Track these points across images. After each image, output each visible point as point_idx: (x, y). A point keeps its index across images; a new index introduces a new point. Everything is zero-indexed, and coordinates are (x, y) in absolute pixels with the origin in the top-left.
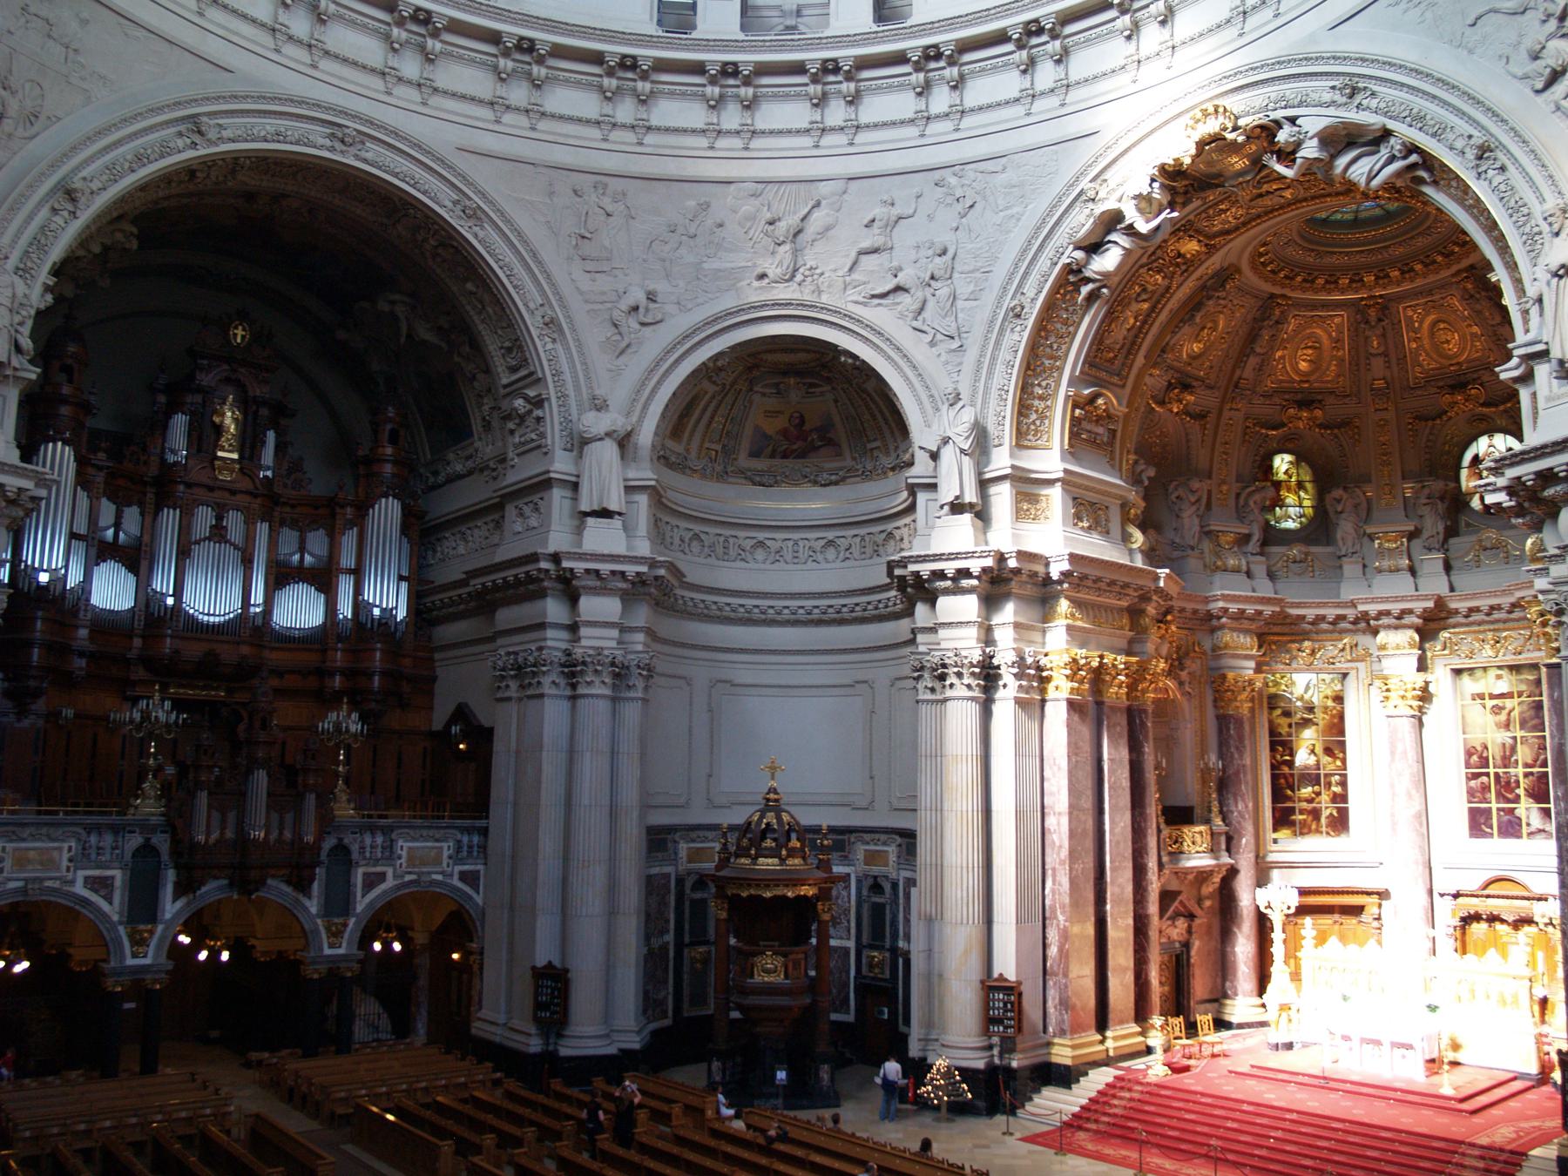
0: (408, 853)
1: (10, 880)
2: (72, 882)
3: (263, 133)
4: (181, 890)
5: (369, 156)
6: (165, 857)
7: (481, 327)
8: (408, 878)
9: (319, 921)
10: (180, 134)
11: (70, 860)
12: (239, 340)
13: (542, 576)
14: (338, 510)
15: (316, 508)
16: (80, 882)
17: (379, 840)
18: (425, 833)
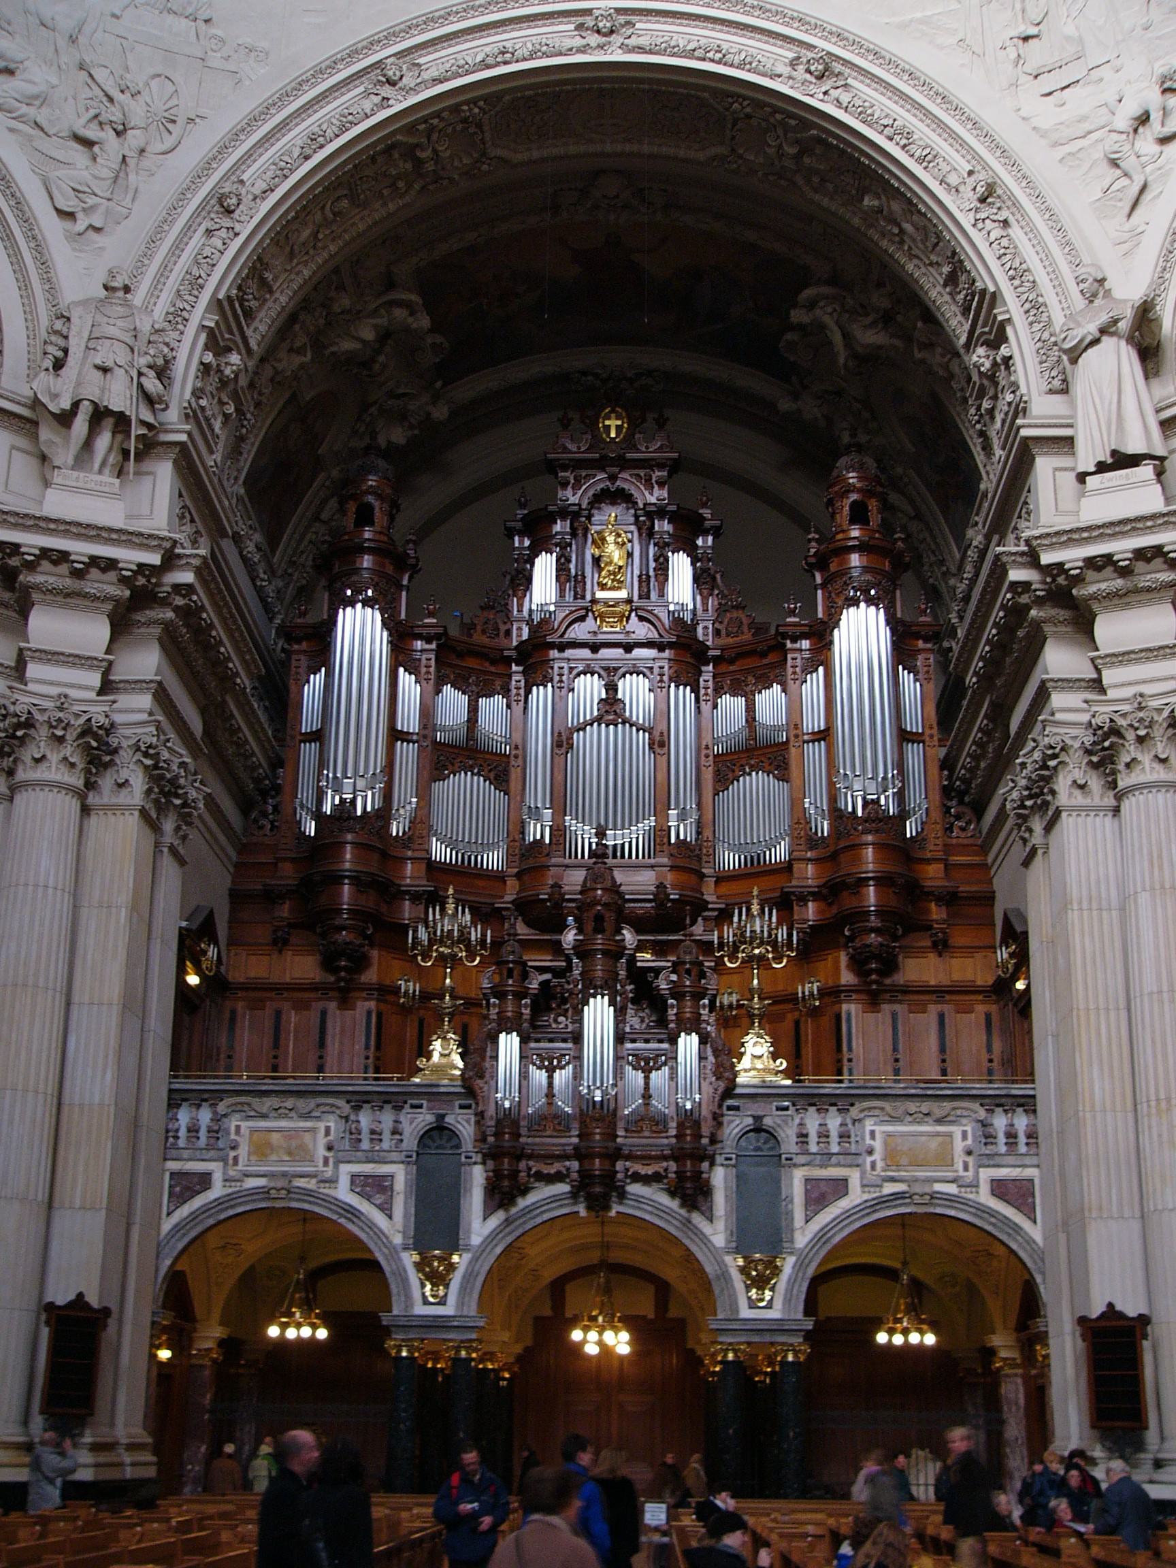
0: (886, 1143)
2: (333, 1181)
3: (479, 59)
5: (643, 41)
7: (910, 267)
8: (889, 1188)
9: (728, 1259)
10: (367, 94)
11: (330, 1148)
12: (613, 435)
13: (1024, 599)
14: (789, 645)
15: (763, 655)
16: (344, 1181)
17: (834, 1122)
18: (912, 1106)
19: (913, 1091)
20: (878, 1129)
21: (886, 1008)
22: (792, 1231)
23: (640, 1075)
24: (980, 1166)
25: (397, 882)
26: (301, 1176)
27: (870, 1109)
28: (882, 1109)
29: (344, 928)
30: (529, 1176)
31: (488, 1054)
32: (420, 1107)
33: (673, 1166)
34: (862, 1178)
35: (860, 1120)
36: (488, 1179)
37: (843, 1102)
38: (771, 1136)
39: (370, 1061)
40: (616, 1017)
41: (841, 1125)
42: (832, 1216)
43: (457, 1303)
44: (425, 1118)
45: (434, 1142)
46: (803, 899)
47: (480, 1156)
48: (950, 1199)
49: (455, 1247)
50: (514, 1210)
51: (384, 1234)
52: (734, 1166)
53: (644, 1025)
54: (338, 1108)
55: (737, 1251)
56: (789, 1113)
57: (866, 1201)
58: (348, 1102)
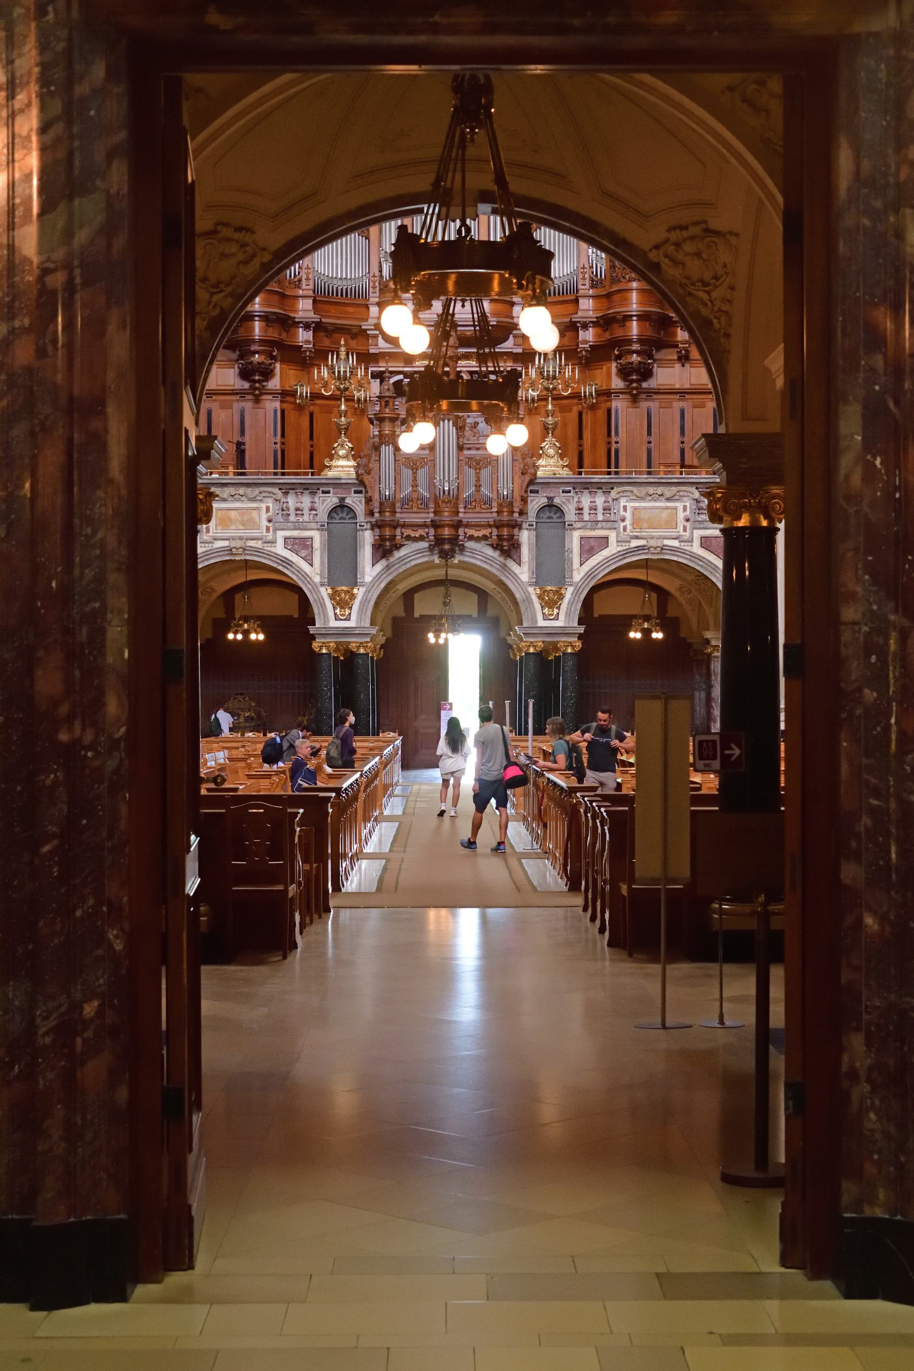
1: (216, 539)
2: (273, 542)
4: (383, 550)
6: (361, 518)
8: (635, 543)
9: (531, 589)
11: (270, 521)
16: (280, 542)
17: (600, 500)
18: (651, 490)
19: (652, 480)
20: (628, 505)
21: (644, 405)
22: (572, 571)
23: (473, 471)
24: (695, 528)
25: (292, 315)
26: (252, 539)
27: (623, 492)
28: (632, 492)
29: (257, 352)
30: (402, 537)
31: (374, 458)
32: (328, 492)
33: (495, 532)
34: (617, 537)
35: (616, 499)
36: (375, 540)
37: (605, 488)
38: (559, 510)
39: (278, 446)
40: (457, 434)
41: (604, 502)
42: (598, 561)
43: (357, 618)
44: (332, 500)
45: (338, 514)
46: (585, 326)
47: (369, 525)
48: (673, 550)
49: (355, 584)
50: (392, 559)
51: (308, 576)
52: (536, 529)
53: (476, 438)
54: (274, 494)
55: (536, 584)
56: (571, 494)
57: (619, 552)
58: (280, 489)
